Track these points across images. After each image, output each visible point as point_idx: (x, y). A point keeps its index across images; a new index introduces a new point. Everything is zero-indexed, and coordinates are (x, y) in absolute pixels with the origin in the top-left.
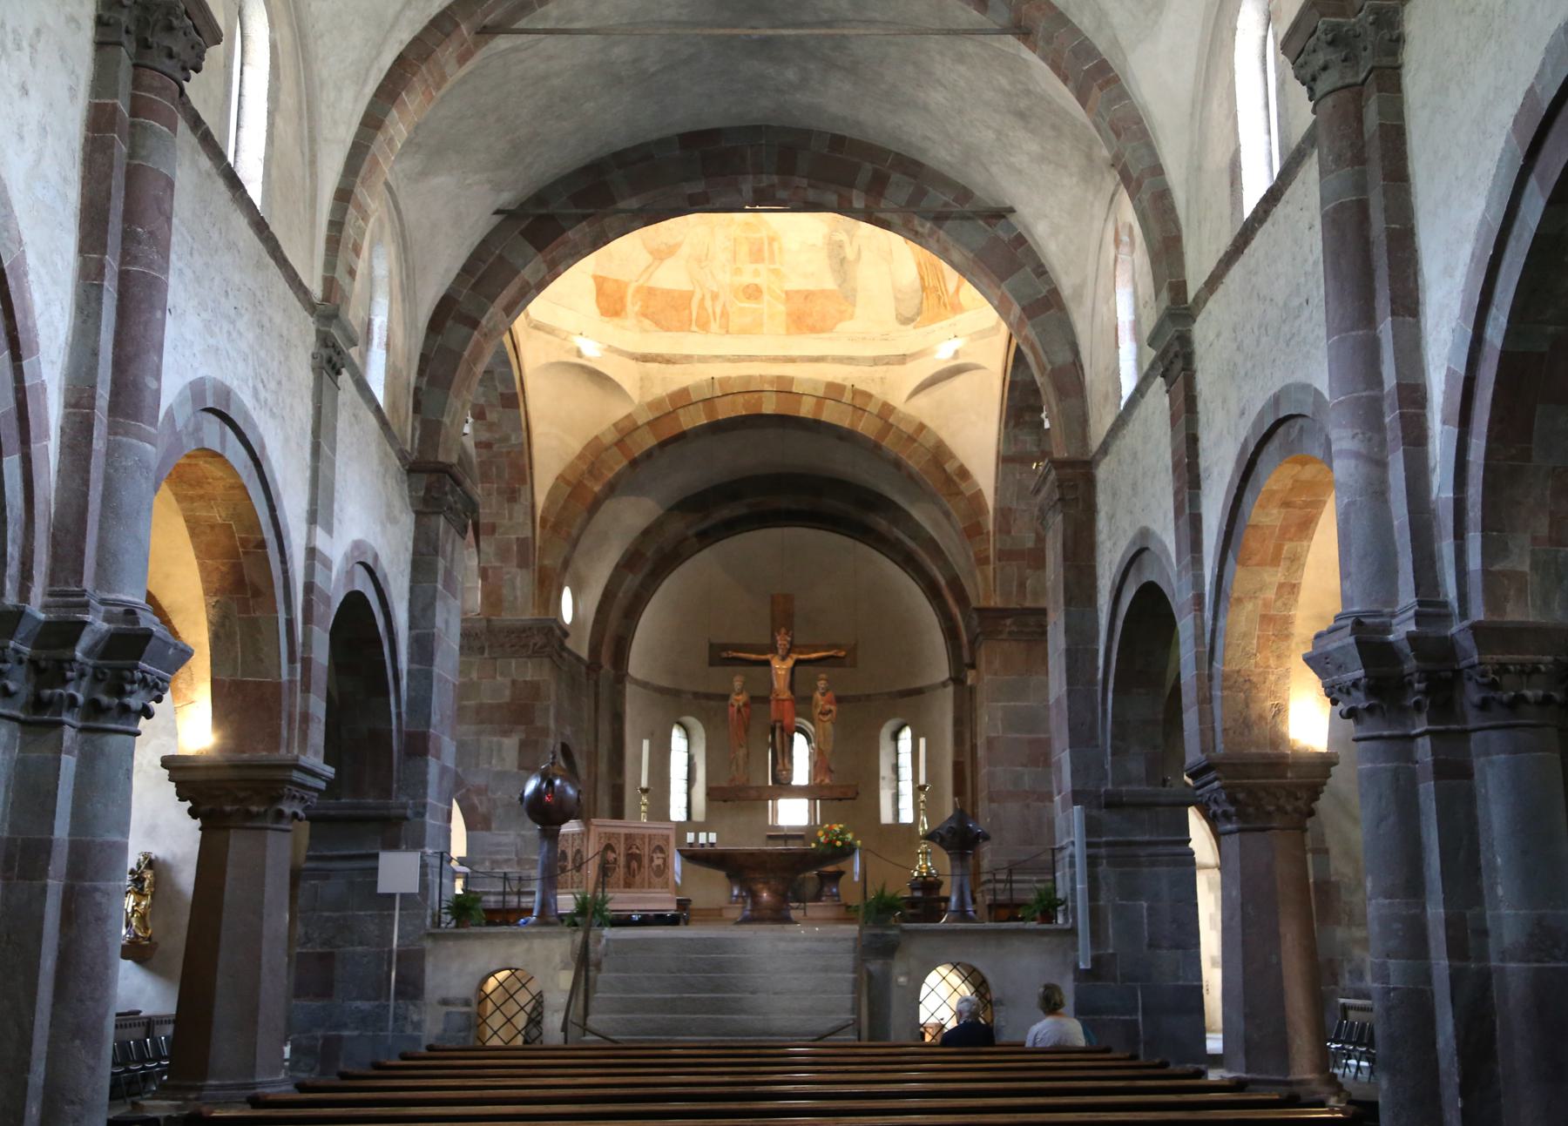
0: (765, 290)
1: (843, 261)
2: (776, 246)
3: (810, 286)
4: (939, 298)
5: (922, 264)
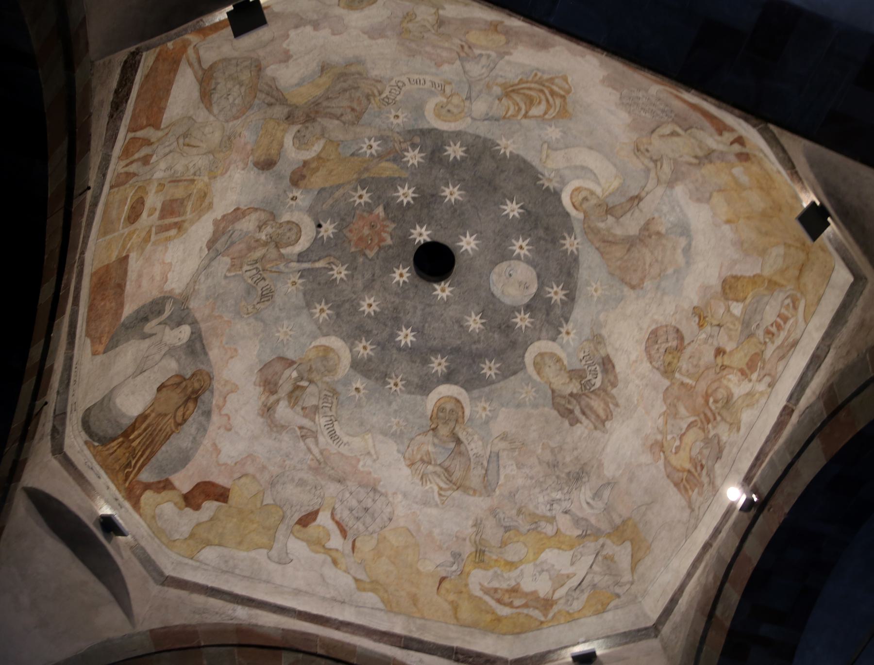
0: (132, 228)
1: (146, 319)
2: (173, 232)
3: (129, 288)
4: (128, 465)
5: (147, 422)
